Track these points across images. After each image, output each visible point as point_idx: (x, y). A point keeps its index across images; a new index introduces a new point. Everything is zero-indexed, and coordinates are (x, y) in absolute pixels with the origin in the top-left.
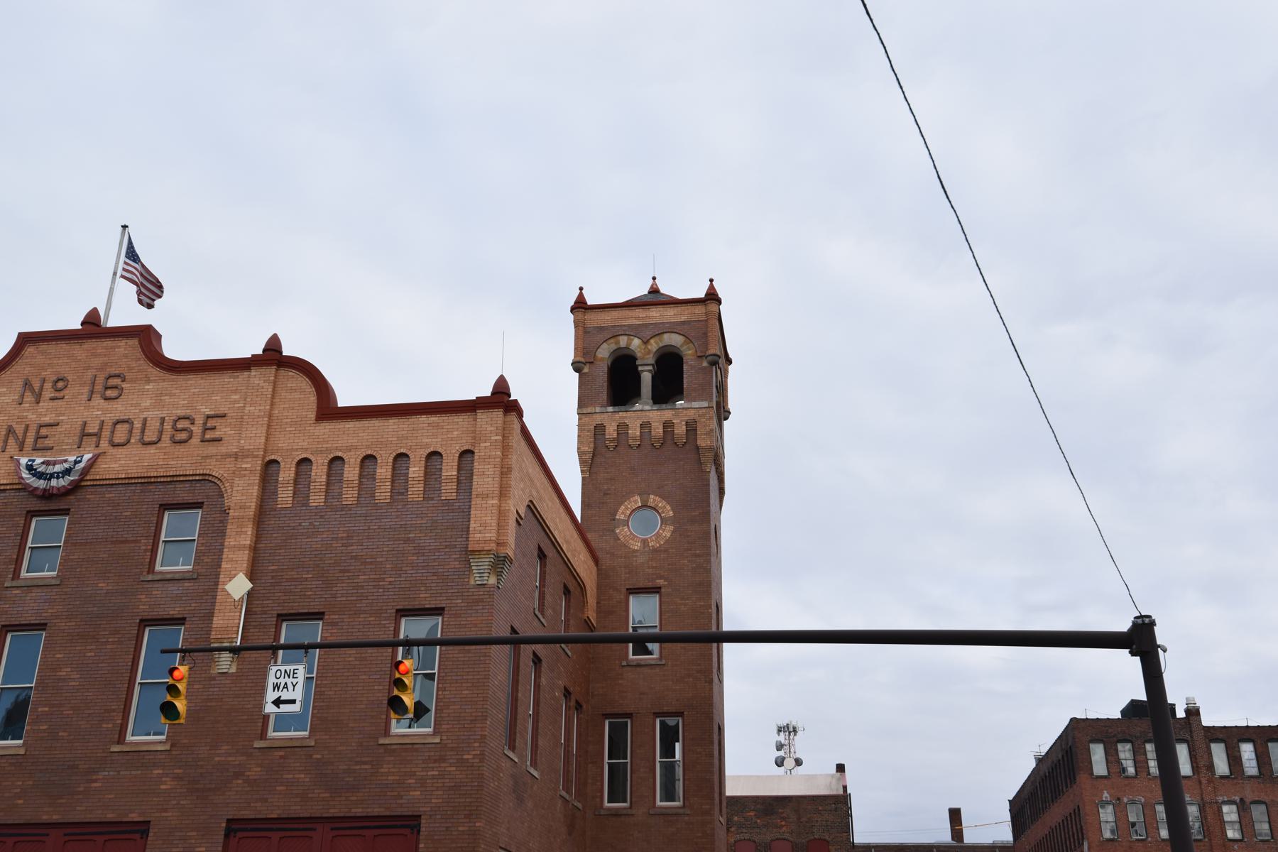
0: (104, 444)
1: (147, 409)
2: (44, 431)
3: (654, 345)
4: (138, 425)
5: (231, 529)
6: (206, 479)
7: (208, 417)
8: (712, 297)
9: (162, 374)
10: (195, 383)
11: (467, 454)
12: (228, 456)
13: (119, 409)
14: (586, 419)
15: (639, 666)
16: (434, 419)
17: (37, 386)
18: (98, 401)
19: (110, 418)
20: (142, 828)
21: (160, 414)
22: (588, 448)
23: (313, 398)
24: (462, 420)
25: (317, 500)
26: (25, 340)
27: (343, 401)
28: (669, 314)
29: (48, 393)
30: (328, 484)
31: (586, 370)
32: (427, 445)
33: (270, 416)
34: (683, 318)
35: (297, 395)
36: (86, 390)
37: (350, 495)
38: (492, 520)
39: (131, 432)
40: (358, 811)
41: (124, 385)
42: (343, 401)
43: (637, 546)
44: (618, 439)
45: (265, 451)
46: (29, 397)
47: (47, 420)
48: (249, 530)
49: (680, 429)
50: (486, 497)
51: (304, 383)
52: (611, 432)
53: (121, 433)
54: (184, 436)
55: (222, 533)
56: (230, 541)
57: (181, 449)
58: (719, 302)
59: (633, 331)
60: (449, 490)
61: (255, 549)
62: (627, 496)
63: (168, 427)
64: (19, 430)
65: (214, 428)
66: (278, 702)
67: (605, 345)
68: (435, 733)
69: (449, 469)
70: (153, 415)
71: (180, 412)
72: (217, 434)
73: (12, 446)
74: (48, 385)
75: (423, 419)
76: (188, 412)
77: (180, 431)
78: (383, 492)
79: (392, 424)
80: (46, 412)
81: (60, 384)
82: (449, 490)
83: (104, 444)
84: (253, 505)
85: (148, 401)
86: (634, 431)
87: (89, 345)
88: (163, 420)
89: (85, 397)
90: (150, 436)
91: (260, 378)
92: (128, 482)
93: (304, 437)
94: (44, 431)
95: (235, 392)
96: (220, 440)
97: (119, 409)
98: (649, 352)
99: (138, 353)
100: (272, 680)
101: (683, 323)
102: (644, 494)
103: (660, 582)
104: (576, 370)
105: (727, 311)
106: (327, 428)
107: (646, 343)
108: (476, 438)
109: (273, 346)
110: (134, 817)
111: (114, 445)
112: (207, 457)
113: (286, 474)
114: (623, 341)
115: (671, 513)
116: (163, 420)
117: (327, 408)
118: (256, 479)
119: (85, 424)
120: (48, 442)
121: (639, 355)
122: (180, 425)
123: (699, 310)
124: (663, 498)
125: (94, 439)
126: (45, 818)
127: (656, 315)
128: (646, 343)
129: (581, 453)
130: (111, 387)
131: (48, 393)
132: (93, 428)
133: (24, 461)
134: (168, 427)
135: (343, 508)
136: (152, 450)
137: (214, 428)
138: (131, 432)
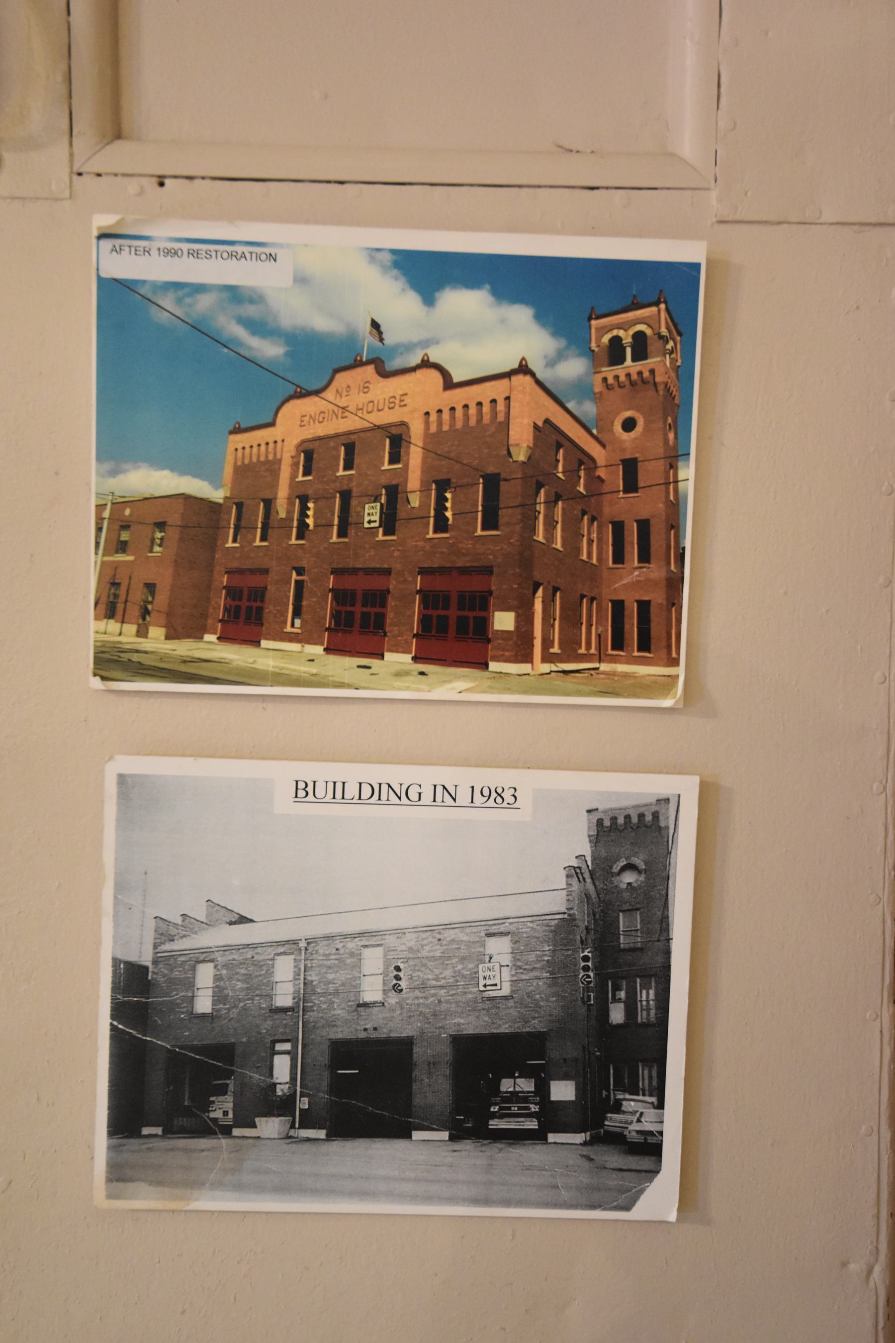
0: (365, 412)
11: (508, 398)
13: (369, 396)
18: (362, 394)
24: (505, 382)
27: (456, 379)
29: (345, 393)
42: (456, 379)
49: (646, 374)
52: (611, 380)
54: (392, 405)
63: (387, 402)
69: (501, 407)
70: (381, 398)
71: (391, 395)
82: (501, 417)
86: (622, 378)
90: (380, 408)
96: (405, 405)
97: (369, 396)
99: (374, 371)
106: (449, 393)
111: (369, 413)
117: (449, 384)
122: (392, 400)
131: (345, 393)
132: (360, 407)
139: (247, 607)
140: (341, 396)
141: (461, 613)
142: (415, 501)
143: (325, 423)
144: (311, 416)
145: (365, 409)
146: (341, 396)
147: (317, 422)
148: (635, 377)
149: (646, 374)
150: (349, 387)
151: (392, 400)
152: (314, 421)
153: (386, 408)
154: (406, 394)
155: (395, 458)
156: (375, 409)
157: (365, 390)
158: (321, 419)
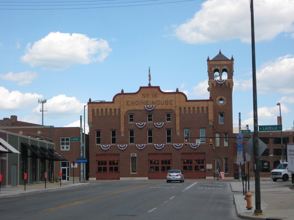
0: (156, 104)
1: (161, 99)
4: (160, 101)
6: (171, 110)
7: (170, 101)
8: (232, 59)
9: (163, 94)
12: (174, 106)
15: (221, 125)
16: (202, 102)
17: (144, 95)
18: (154, 98)
19: (156, 100)
20: (171, 154)
23: (185, 98)
24: (206, 102)
25: (187, 113)
26: (141, 88)
28: (225, 62)
29: (146, 96)
31: (210, 73)
32: (201, 106)
34: (227, 63)
35: (182, 98)
36: (152, 96)
37: (192, 112)
39: (159, 103)
40: (197, 152)
41: (157, 95)
43: (220, 105)
49: (227, 84)
51: (183, 96)
54: (167, 103)
56: (177, 119)
59: (218, 65)
60: (205, 112)
63: (165, 102)
64: (143, 101)
65: (171, 102)
66: (197, 143)
67: (213, 68)
68: (206, 143)
69: (205, 110)
71: (166, 100)
72: (172, 103)
73: (143, 105)
74: (146, 95)
75: (201, 102)
76: (167, 100)
77: (167, 102)
78: (196, 112)
79: (196, 103)
81: (148, 95)
82: (205, 112)
83: (156, 104)
87: (151, 89)
88: (164, 101)
89: (152, 97)
91: (177, 95)
92: (160, 110)
94: (147, 102)
95: (173, 97)
96: (172, 104)
97: (157, 99)
100: (196, 141)
103: (224, 111)
104: (208, 72)
105: (234, 62)
106: (187, 103)
107: (221, 68)
109: (177, 90)
110: (170, 152)
112: (171, 106)
113: (183, 109)
114: (216, 67)
115: (226, 99)
116: (164, 101)
119: (153, 101)
120: (148, 103)
121: (219, 70)
123: (230, 62)
125: (154, 103)
126: (158, 153)
127: (222, 62)
128: (221, 68)
130: (155, 96)
131: (146, 96)
132: (154, 102)
133: (146, 106)
134: (165, 102)
136: (163, 105)
137: (171, 102)
138: (159, 103)
139: (162, 167)
140: (145, 97)
141: (110, 166)
143: (139, 105)
145: (156, 103)
147: (135, 104)
149: (227, 84)
150: (148, 94)
152: (134, 104)
153: (165, 104)
154: (172, 101)
156: (160, 104)
157: (155, 96)
158: (136, 104)
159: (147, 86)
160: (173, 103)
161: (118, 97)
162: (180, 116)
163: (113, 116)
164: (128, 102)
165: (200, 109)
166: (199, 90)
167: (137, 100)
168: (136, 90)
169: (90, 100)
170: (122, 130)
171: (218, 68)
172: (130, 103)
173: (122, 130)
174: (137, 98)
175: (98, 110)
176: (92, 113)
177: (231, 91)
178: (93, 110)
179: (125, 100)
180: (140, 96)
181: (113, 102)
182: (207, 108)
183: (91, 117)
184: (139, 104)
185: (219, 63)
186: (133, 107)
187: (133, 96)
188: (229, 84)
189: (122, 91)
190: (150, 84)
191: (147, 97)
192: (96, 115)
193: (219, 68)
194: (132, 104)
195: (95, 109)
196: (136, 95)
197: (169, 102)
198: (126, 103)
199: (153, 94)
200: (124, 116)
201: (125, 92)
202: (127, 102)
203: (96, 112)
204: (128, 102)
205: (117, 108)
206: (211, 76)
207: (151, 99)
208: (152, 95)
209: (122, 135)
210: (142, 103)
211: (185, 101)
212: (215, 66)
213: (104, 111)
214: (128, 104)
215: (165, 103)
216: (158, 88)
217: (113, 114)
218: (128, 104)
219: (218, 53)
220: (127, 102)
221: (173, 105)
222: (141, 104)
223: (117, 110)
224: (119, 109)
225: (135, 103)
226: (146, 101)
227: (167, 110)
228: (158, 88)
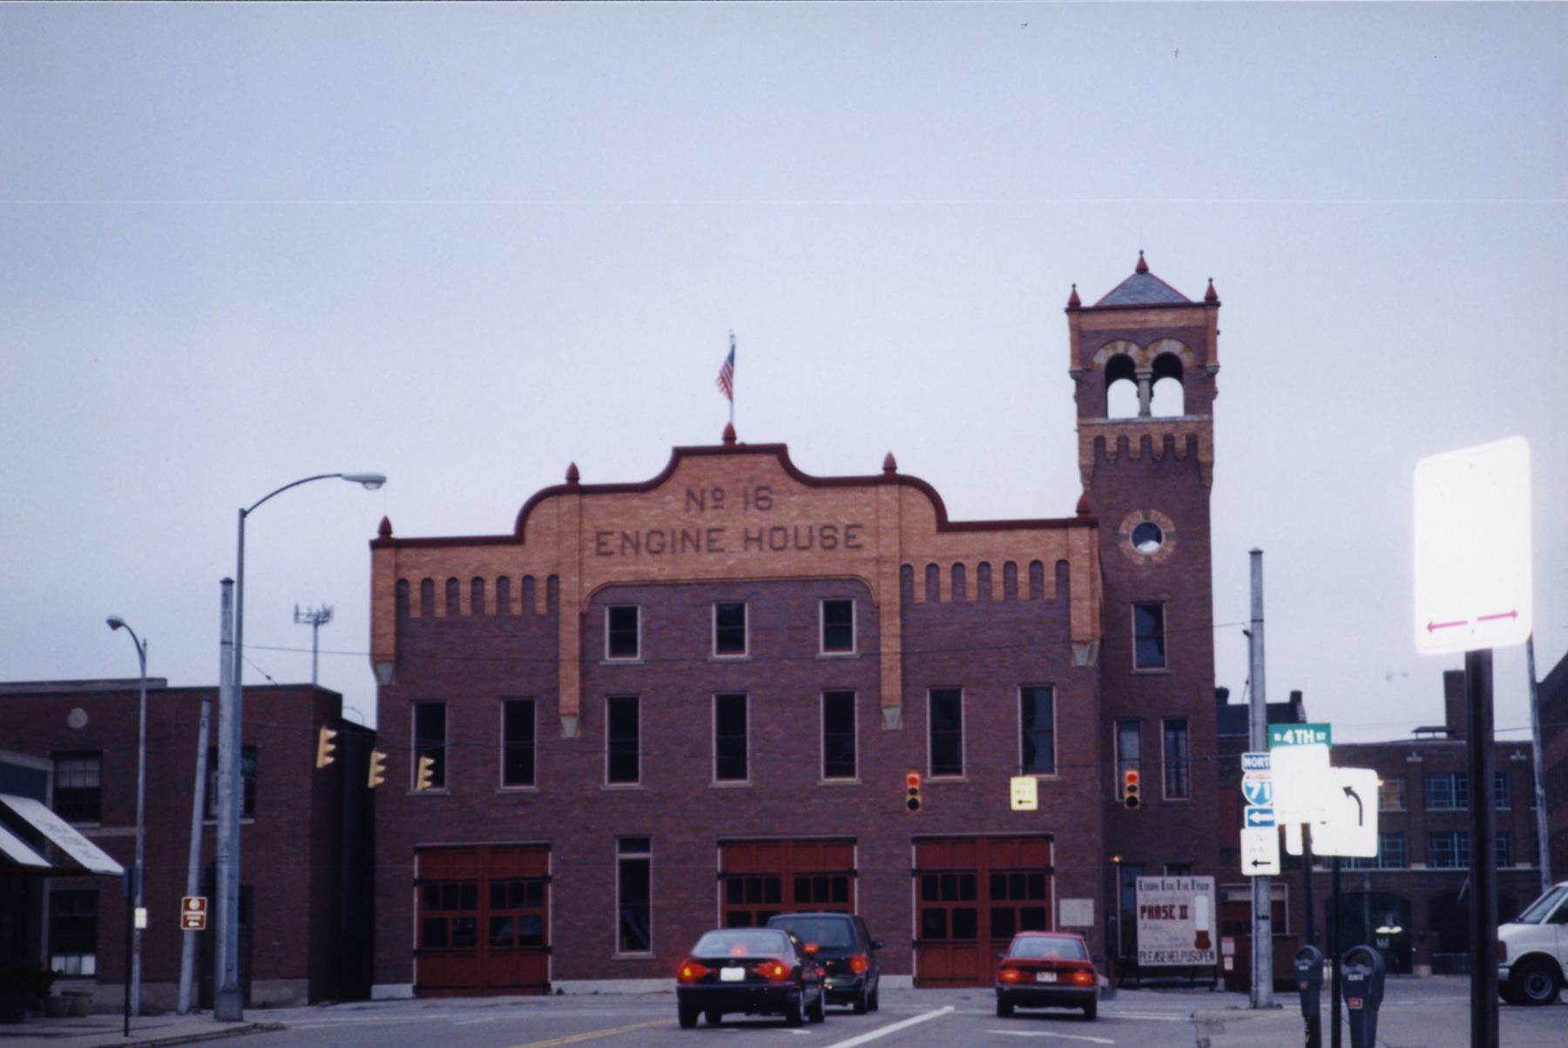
2: (714, 535)
3: (1152, 355)
4: (791, 532)
5: (884, 622)
6: (854, 579)
7: (849, 527)
8: (1212, 301)
9: (804, 488)
10: (832, 497)
12: (867, 560)
14: (1085, 431)
16: (1033, 533)
17: (698, 495)
18: (752, 510)
19: (767, 525)
21: (810, 522)
22: (1090, 462)
23: (930, 512)
24: (1055, 535)
25: (946, 597)
26: (680, 454)
28: (1168, 319)
29: (709, 503)
30: (954, 584)
33: (900, 528)
34: (1182, 323)
36: (741, 499)
37: (972, 594)
38: (1087, 618)
41: (774, 497)
42: (954, 516)
43: (1140, 561)
44: (1118, 453)
45: (901, 557)
46: (694, 506)
47: (713, 525)
48: (898, 621)
49: (1181, 444)
50: (1079, 599)
51: (922, 499)
53: (778, 539)
54: (830, 542)
55: (878, 626)
56: (884, 631)
57: (830, 554)
58: (1218, 305)
59: (1131, 336)
60: (1050, 592)
61: (902, 637)
62: (1129, 511)
63: (816, 534)
64: (693, 533)
69: (1050, 576)
71: (825, 522)
72: (857, 542)
74: (708, 495)
77: (828, 538)
78: (998, 592)
79: (999, 537)
80: (708, 519)
81: (718, 495)
84: (897, 600)
85: (793, 511)
87: (736, 459)
89: (741, 506)
90: (804, 542)
91: (886, 494)
93: (930, 548)
95: (867, 505)
96: (858, 547)
97: (772, 519)
98: (1147, 359)
99: (778, 465)
101: (1182, 328)
102: (1146, 509)
106: (946, 539)
108: (1069, 551)
109: (890, 465)
113: (920, 577)
114: (1121, 347)
116: (811, 528)
117: (944, 526)
118: (896, 581)
119: (746, 531)
120: (718, 545)
121: (1137, 362)
122: (828, 532)
123: (1198, 317)
124: (1166, 513)
127: (1154, 319)
129: (1082, 467)
131: (709, 503)
132: (755, 535)
134: (816, 534)
135: (968, 604)
136: (806, 554)
140: (702, 507)
142: (892, 718)
143: (667, 555)
144: (625, 537)
145: (766, 538)
146: (702, 507)
147: (643, 550)
148: (1159, 444)
149: (1181, 444)
150: (718, 490)
151: (828, 532)
152: (637, 547)
154: (859, 526)
155: (838, 633)
157: (761, 503)
158: (654, 546)
159: (717, 440)
160: (862, 538)
161: (546, 508)
162: (903, 614)
163: (518, 617)
164: (603, 539)
165: (1023, 576)
166: (1012, 459)
167: (654, 525)
168: (651, 466)
169: (386, 527)
170: (569, 697)
171: (1127, 349)
172: (613, 542)
173: (569, 697)
174: (655, 512)
175: (427, 582)
176: (392, 600)
177: (1201, 479)
178: (402, 584)
179: (586, 526)
180: (672, 500)
181: (518, 539)
182: (1062, 565)
183: (389, 628)
184: (668, 549)
185: (1135, 322)
186: (633, 568)
187: (635, 501)
188: (1193, 442)
189: (573, 473)
190: (730, 434)
191: (715, 507)
192: (416, 613)
193: (1133, 351)
194: (630, 550)
195: (415, 577)
196: (654, 494)
197: (841, 537)
198: (593, 545)
199: (751, 490)
200: (583, 616)
201: (584, 480)
202: (599, 534)
203: (415, 594)
204: (603, 539)
205: (541, 572)
206: (1090, 400)
207: (739, 520)
208: (746, 495)
209: (570, 728)
210: (688, 543)
211: (933, 526)
212: (1113, 341)
213: (465, 589)
214: (603, 549)
215: (817, 543)
216: (780, 451)
217: (516, 609)
218: (603, 549)
219: (1131, 270)
220: (599, 534)
221: (864, 554)
222: (678, 547)
223: (541, 586)
224: (553, 579)
225: (643, 540)
226: (710, 531)
227: (829, 579)
228: (780, 451)
